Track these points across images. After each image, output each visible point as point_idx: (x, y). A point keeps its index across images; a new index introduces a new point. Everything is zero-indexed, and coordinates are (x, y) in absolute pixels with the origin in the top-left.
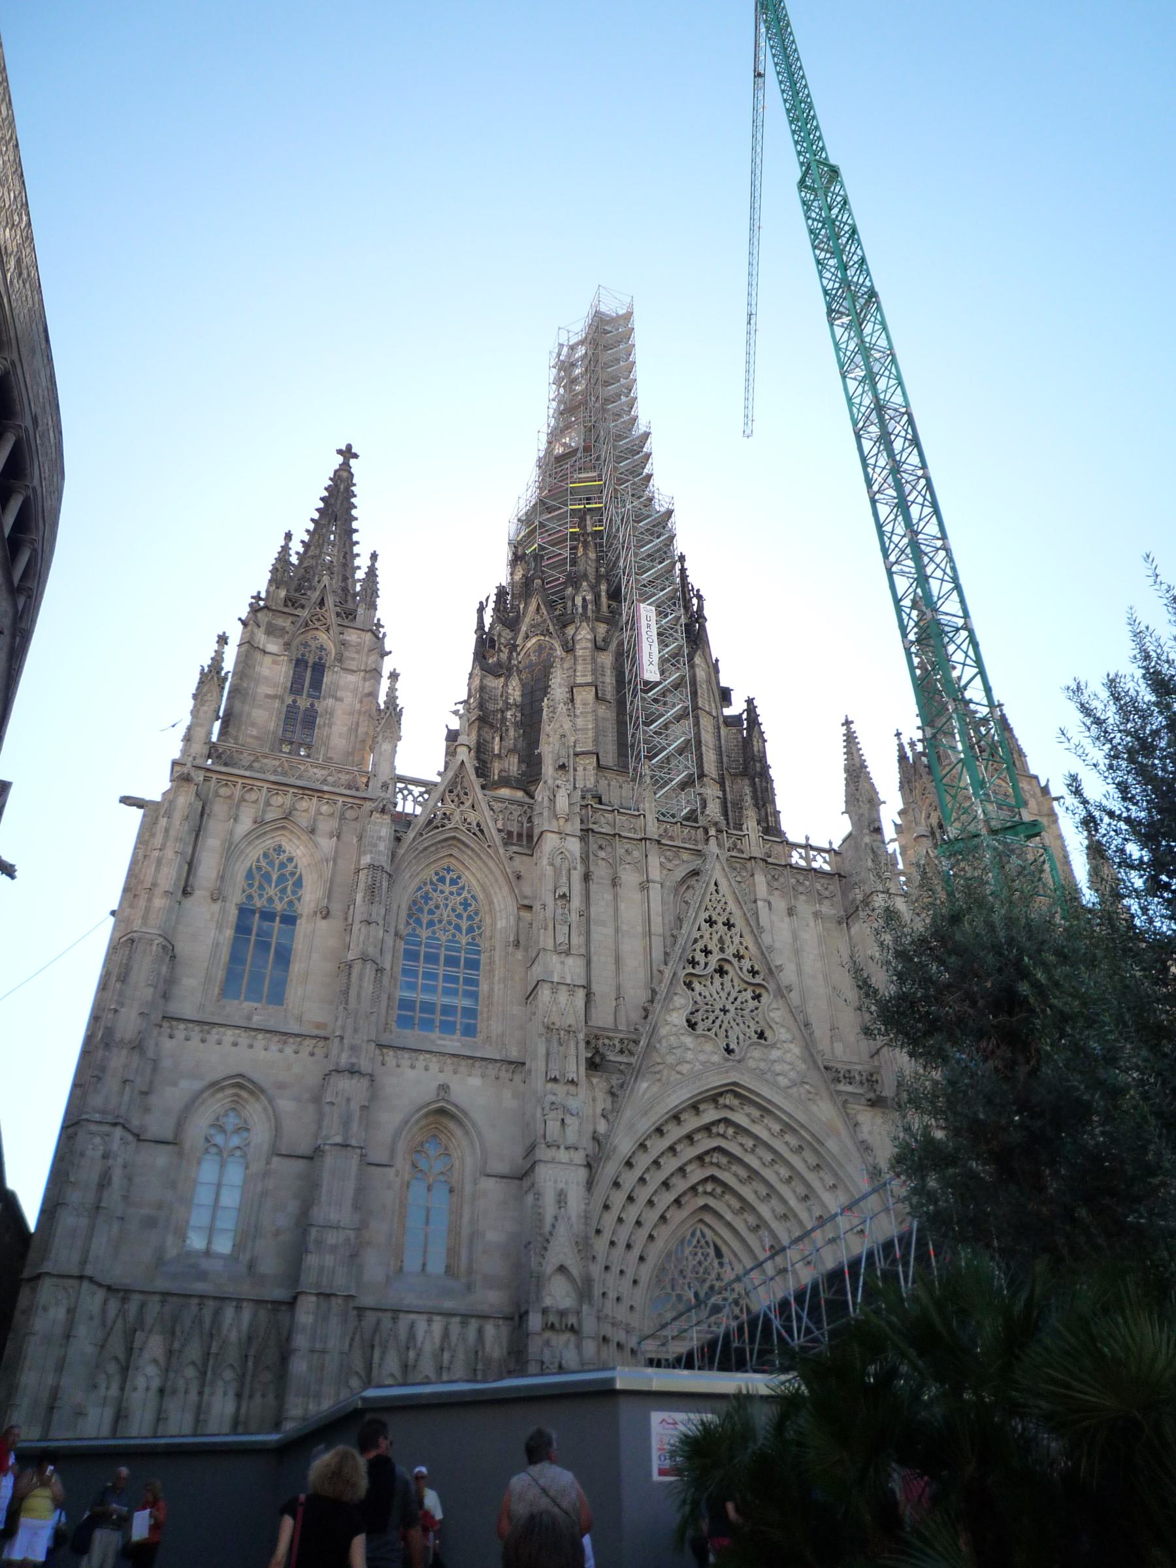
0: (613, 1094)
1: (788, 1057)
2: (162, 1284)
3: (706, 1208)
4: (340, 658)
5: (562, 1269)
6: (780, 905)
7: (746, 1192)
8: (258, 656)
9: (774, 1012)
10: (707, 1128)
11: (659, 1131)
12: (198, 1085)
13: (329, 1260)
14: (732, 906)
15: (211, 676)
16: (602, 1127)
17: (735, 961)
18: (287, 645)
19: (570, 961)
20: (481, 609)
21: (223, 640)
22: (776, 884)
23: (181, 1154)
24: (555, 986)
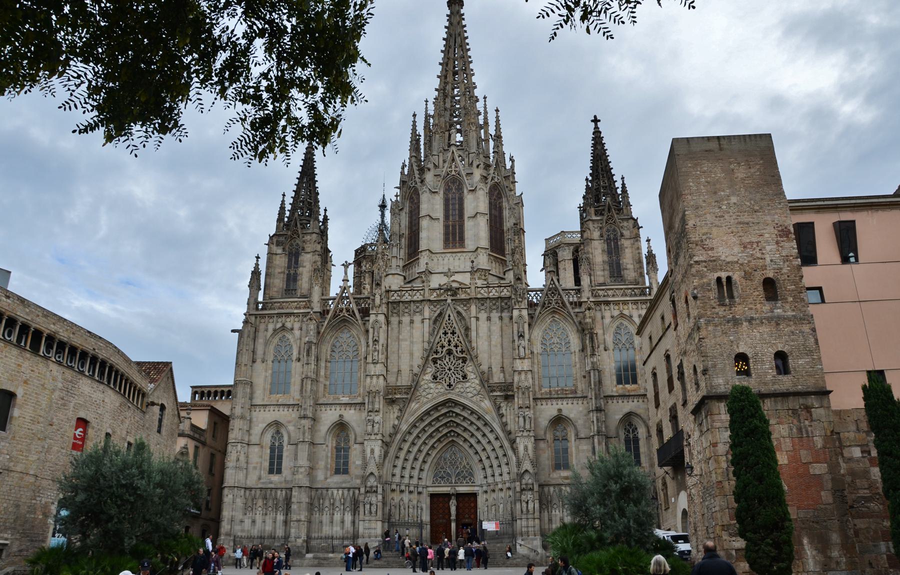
0: (400, 410)
1: (473, 385)
2: (260, 486)
3: (453, 441)
4: (303, 249)
5: (372, 474)
6: (483, 316)
7: (466, 435)
8: (274, 256)
9: (469, 369)
10: (445, 414)
11: (421, 419)
12: (265, 425)
13: (301, 476)
14: (455, 325)
15: (256, 273)
16: (396, 422)
17: (454, 349)
18: (284, 249)
19: (378, 365)
20: (403, 168)
21: (258, 258)
22: (483, 307)
23: (262, 447)
24: (372, 377)
